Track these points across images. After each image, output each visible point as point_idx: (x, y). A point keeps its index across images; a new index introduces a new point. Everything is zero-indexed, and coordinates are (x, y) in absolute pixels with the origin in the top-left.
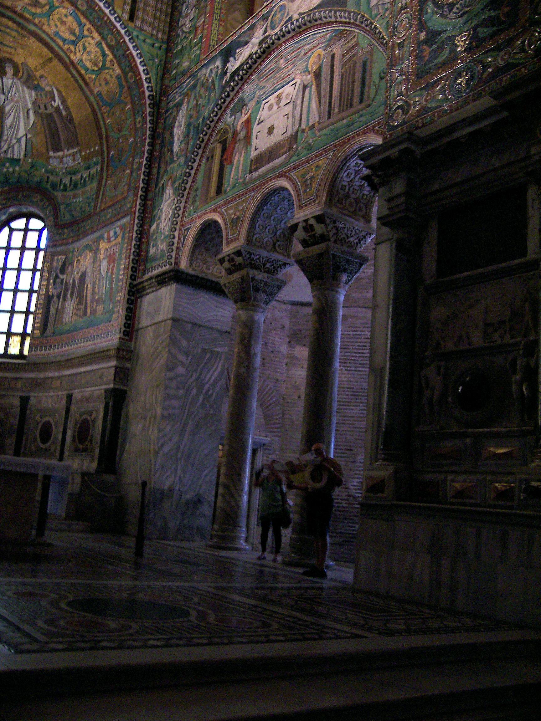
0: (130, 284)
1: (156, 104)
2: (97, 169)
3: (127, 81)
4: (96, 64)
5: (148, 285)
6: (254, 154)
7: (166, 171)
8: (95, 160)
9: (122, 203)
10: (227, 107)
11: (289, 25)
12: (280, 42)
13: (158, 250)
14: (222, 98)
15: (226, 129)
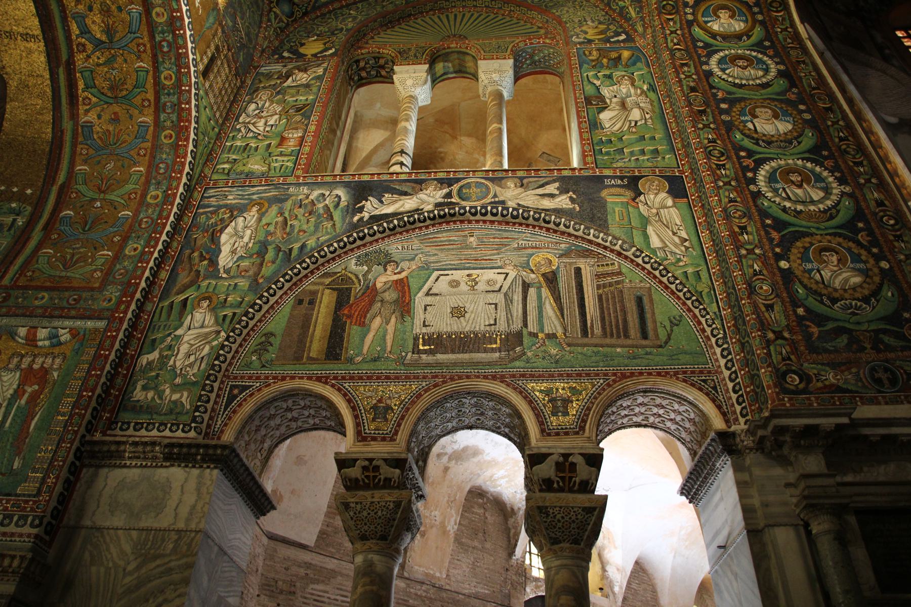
0: (83, 436)
1: (189, 189)
2: (14, 220)
3: (156, 137)
4: (112, 88)
5: (130, 452)
6: (418, 329)
7: (194, 282)
8: (14, 205)
9: (84, 295)
10: (352, 250)
11: (500, 209)
12: (472, 218)
13: (160, 398)
14: (352, 235)
15: (350, 278)
